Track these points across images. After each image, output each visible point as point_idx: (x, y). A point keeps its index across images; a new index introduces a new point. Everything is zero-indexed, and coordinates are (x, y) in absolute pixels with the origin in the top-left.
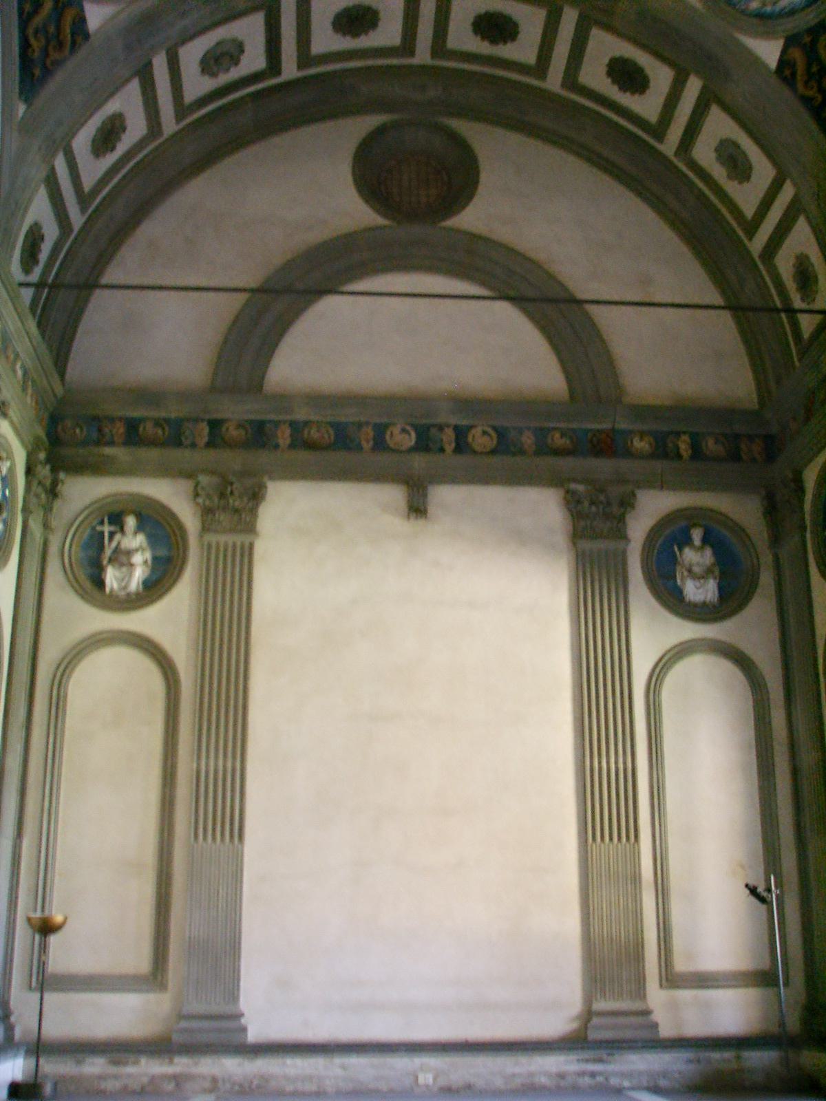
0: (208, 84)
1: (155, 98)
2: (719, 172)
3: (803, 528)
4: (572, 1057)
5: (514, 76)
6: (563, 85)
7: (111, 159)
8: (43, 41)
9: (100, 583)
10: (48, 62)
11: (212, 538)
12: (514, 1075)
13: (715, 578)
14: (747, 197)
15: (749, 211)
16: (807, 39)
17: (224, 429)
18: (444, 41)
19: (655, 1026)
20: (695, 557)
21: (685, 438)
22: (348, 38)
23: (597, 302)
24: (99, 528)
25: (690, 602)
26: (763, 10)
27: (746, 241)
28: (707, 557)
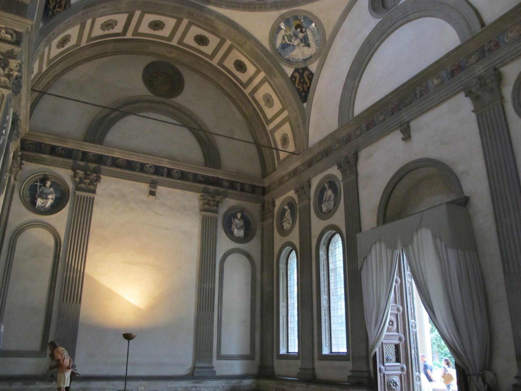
0: (101, 33)
1: (83, 33)
2: (262, 103)
3: (273, 217)
4: (190, 382)
5: (203, 57)
6: (218, 64)
7: (62, 49)
9: (34, 203)
11: (78, 193)
12: (171, 387)
13: (243, 229)
14: (270, 113)
15: (269, 117)
16: (301, 71)
17: (88, 154)
18: (183, 40)
19: (215, 372)
20: (237, 222)
21: (239, 184)
22: (152, 30)
23: (217, 135)
24: (36, 183)
25: (235, 236)
27: (266, 125)
28: (241, 223)
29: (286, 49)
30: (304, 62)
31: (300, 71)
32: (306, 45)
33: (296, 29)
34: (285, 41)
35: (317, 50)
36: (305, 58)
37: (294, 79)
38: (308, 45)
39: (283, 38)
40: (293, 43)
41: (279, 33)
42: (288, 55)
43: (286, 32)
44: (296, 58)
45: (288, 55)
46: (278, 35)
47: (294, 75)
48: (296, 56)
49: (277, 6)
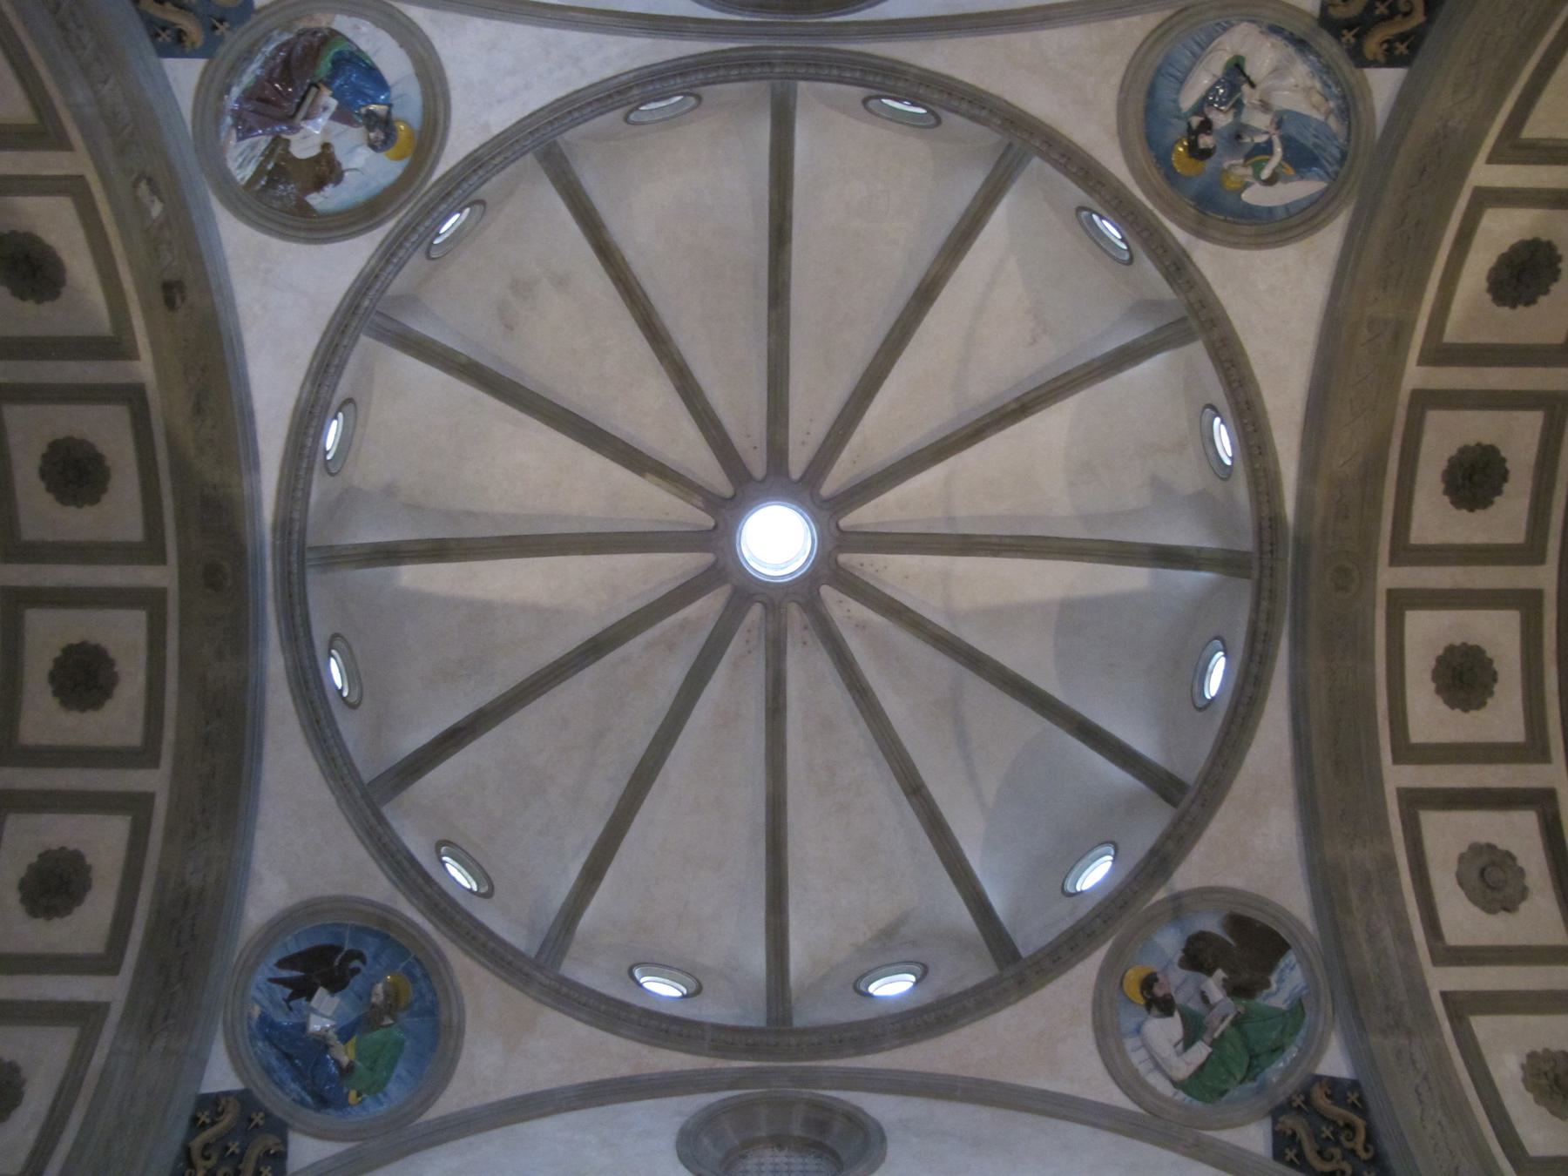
8: (1337, 1152)
10: (1364, 1155)
16: (1349, 36)
26: (1336, 111)
29: (1309, 141)
30: (1312, 44)
31: (1353, 40)
32: (1242, 78)
33: (1206, 154)
34: (1280, 164)
35: (1234, 22)
36: (1291, 50)
37: (1397, 44)
38: (1236, 71)
39: (1270, 181)
40: (1272, 130)
41: (1266, 204)
42: (1325, 124)
43: (1248, 180)
44: (1318, 85)
45: (1325, 124)
46: (1276, 207)
47: (1381, 58)
48: (1308, 91)
49: (1175, 264)
